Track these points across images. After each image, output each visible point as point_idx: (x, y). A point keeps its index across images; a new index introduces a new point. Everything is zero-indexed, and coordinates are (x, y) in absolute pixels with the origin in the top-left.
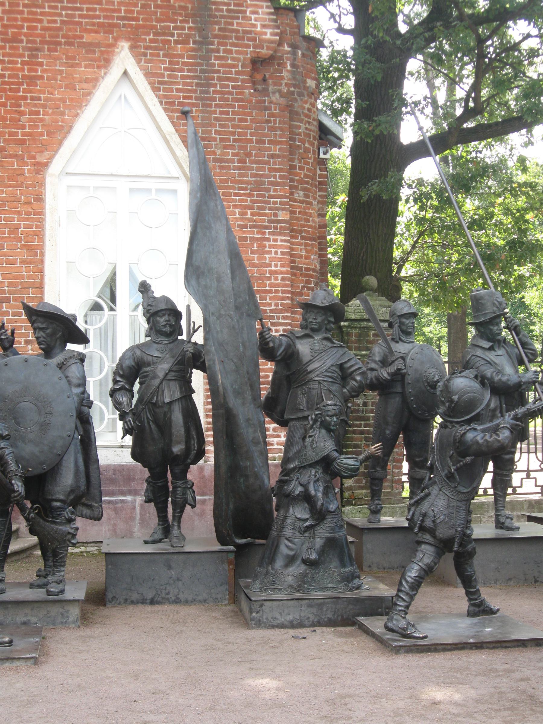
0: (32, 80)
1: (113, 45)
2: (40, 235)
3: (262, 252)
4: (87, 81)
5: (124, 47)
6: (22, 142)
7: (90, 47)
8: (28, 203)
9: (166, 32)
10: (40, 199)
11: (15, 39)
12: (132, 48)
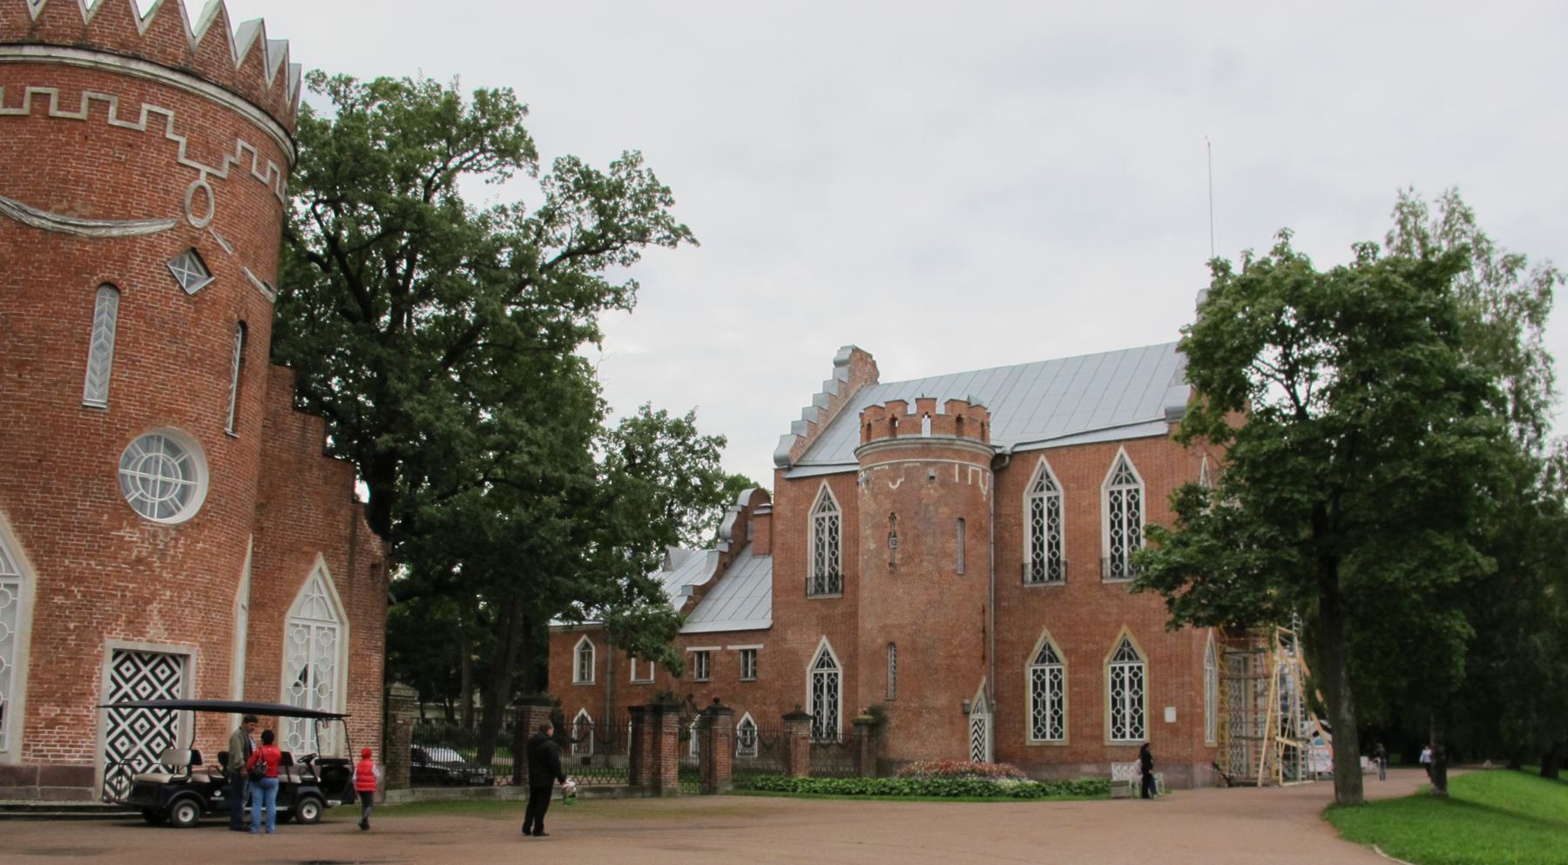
0: (281, 569)
1: (315, 554)
2: (280, 648)
3: (370, 661)
4: (303, 571)
5: (320, 554)
6: (274, 600)
7: (306, 554)
8: (275, 631)
9: (337, 549)
10: (281, 630)
11: (275, 547)
12: (324, 555)
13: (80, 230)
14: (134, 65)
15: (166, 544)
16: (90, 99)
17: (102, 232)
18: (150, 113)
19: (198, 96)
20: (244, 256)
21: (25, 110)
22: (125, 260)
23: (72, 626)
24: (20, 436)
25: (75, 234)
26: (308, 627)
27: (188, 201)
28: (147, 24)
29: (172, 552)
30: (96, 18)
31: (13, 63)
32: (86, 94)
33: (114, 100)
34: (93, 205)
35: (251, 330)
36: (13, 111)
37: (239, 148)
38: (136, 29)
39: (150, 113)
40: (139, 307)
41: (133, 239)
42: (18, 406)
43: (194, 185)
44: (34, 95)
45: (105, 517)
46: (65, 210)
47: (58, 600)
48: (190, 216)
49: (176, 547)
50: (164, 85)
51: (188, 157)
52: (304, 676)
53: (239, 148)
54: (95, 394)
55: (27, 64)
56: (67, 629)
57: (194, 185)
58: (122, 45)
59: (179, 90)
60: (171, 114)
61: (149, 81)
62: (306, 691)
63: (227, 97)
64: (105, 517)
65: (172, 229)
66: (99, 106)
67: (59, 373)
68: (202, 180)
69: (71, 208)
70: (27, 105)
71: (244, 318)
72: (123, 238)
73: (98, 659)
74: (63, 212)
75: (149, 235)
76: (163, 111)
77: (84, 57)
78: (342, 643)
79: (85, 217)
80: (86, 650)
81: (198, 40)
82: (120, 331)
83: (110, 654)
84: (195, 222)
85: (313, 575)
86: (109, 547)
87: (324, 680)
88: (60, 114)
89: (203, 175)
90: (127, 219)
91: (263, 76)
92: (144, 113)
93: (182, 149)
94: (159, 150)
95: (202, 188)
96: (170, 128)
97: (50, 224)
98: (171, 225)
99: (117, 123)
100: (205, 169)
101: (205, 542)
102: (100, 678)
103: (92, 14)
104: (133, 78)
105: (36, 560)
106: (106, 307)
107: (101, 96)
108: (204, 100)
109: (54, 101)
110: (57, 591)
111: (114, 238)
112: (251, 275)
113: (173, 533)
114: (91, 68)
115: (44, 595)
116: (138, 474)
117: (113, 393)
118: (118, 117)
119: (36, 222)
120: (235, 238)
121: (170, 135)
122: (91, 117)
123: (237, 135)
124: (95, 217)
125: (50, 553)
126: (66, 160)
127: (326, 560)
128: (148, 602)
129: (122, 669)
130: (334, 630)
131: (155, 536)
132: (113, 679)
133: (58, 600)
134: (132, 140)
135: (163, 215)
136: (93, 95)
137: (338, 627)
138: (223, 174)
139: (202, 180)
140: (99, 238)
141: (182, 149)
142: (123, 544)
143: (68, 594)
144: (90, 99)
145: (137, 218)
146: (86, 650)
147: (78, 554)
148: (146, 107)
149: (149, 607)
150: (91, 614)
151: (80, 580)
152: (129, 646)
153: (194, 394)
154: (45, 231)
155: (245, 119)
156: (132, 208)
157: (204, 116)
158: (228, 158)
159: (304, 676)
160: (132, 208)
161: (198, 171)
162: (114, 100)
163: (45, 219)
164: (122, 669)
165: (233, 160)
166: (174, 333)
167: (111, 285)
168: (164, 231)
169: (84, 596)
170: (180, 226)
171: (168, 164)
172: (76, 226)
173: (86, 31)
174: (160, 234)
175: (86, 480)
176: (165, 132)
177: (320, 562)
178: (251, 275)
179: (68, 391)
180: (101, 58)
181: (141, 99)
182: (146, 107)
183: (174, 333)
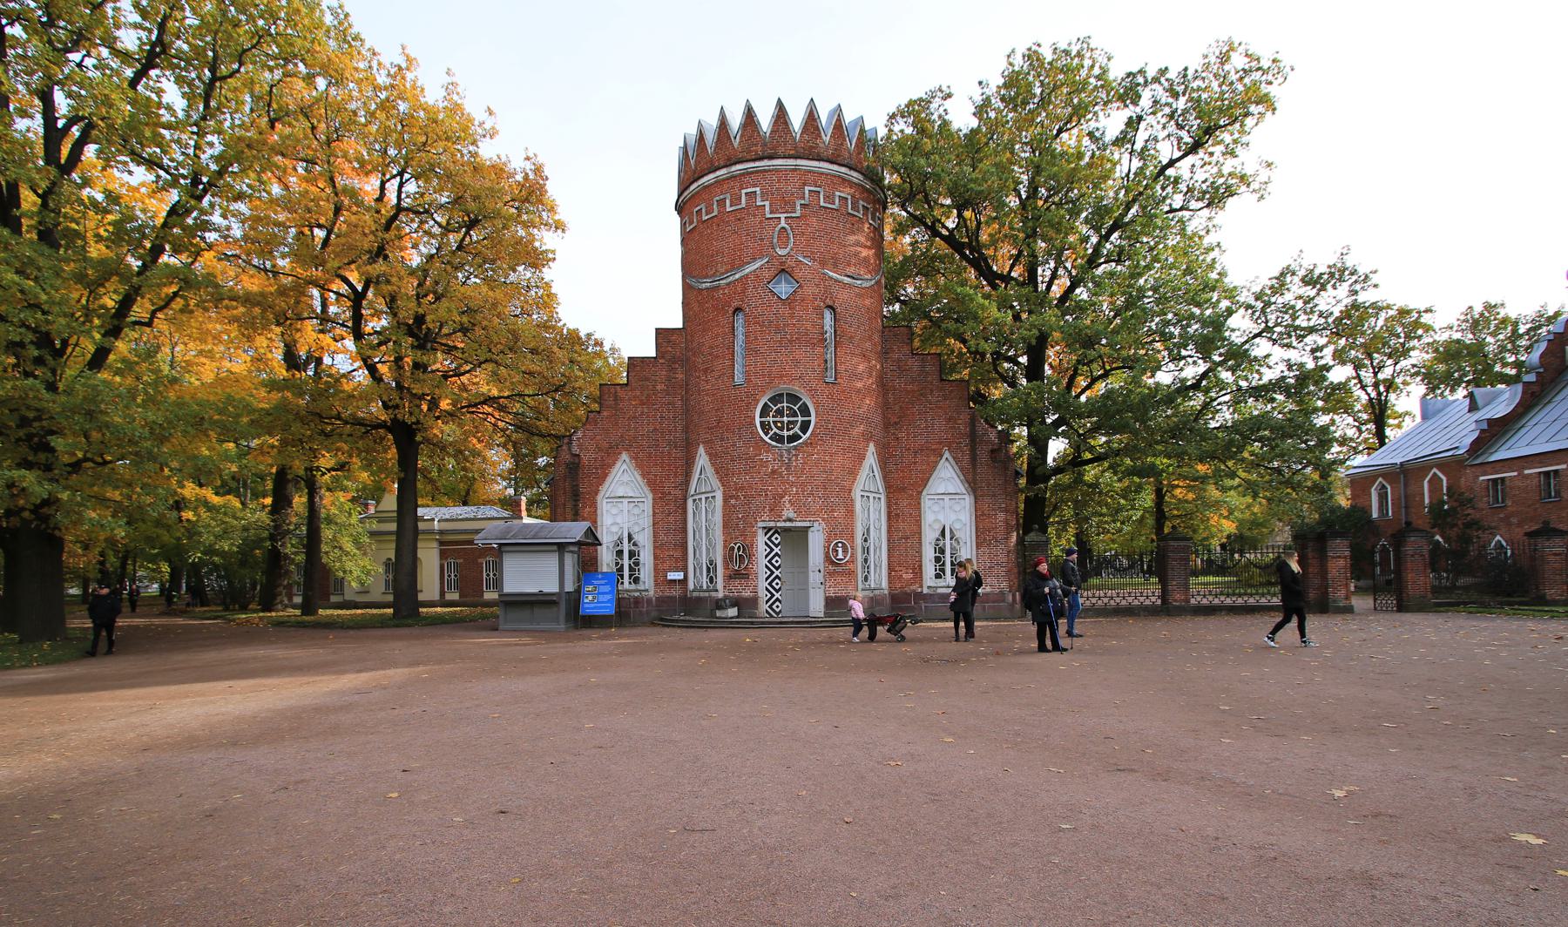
14: (734, 168)
15: (789, 460)
17: (731, 279)
19: (773, 170)
20: (823, 264)
22: (744, 290)
27: (775, 241)
28: (738, 137)
33: (728, 196)
35: (838, 310)
37: (807, 192)
42: (707, 395)
43: (777, 229)
47: (733, 502)
48: (778, 250)
49: (797, 460)
50: (752, 173)
53: (807, 192)
54: (739, 378)
56: (738, 518)
57: (777, 229)
58: (729, 159)
60: (758, 189)
63: (791, 162)
66: (722, 203)
68: (783, 223)
71: (829, 302)
72: (741, 278)
73: (755, 534)
74: (714, 275)
75: (755, 271)
76: (754, 189)
79: (723, 274)
81: (768, 134)
84: (780, 252)
89: (783, 221)
90: (742, 266)
91: (821, 137)
92: (743, 195)
93: (767, 209)
94: (755, 216)
95: (783, 228)
96: (759, 199)
100: (783, 216)
101: (818, 454)
104: (735, 177)
106: (740, 321)
107: (722, 197)
108: (777, 171)
112: (831, 274)
113: (794, 452)
114: (716, 182)
115: (726, 500)
116: (771, 419)
117: (747, 374)
119: (704, 285)
120: (812, 253)
122: (719, 212)
123: (805, 184)
126: (712, 244)
131: (782, 456)
133: (733, 502)
134: (739, 216)
136: (718, 198)
138: (798, 214)
139: (783, 223)
140: (730, 283)
141: (767, 209)
142: (764, 464)
143: (737, 498)
145: (750, 263)
148: (744, 191)
151: (742, 488)
152: (772, 524)
153: (797, 362)
154: (707, 288)
155: (810, 172)
157: (779, 181)
158: (798, 203)
164: (773, 539)
165: (803, 202)
166: (777, 327)
167: (738, 310)
170: (772, 258)
171: (761, 222)
173: (711, 161)
178: (831, 274)
180: (718, 173)
183: (777, 327)
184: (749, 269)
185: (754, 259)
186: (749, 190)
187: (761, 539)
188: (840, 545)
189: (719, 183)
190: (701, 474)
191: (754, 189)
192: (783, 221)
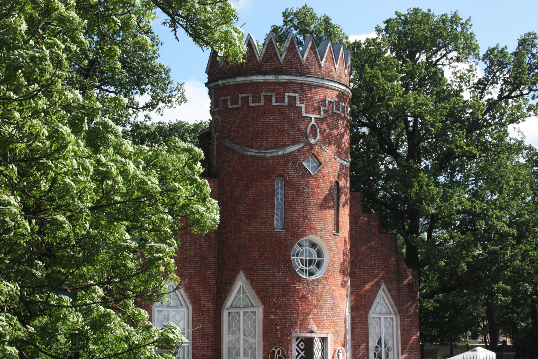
2: (367, 329)
10: (367, 321)
12: (384, 282)
13: (266, 154)
14: (280, 77)
16: (264, 96)
18: (289, 97)
21: (240, 105)
22: (285, 164)
23: (278, 328)
24: (251, 247)
25: (264, 157)
26: (380, 318)
29: (316, 292)
30: (263, 59)
31: (233, 85)
32: (263, 94)
33: (274, 94)
34: (270, 143)
36: (235, 106)
38: (279, 60)
39: (289, 97)
40: (293, 184)
41: (288, 155)
44: (242, 98)
45: (288, 279)
46: (260, 146)
47: (272, 317)
49: (318, 289)
50: (293, 83)
51: (306, 113)
52: (380, 342)
55: (238, 86)
56: (277, 329)
58: (275, 69)
59: (299, 83)
61: (286, 83)
62: (381, 350)
64: (288, 279)
65: (303, 147)
66: (268, 99)
67: (263, 218)
68: (313, 122)
69: (262, 145)
70: (240, 103)
73: (290, 342)
75: (294, 152)
76: (294, 95)
77: (260, 78)
78: (397, 325)
79: (268, 149)
80: (285, 338)
82: (286, 195)
83: (294, 340)
85: (381, 292)
86: (290, 292)
87: (390, 344)
88: (253, 105)
89: (313, 120)
93: (303, 110)
94: (294, 113)
96: (298, 102)
97: (254, 154)
98: (302, 145)
99: (276, 104)
100: (313, 116)
102: (291, 350)
103: (261, 58)
105: (262, 299)
107: (268, 94)
109: (250, 99)
110: (272, 313)
111: (280, 156)
118: (276, 102)
121: (297, 105)
124: (271, 148)
125: (267, 297)
127: (385, 284)
128: (308, 315)
129: (300, 345)
130: (392, 318)
132: (297, 350)
133: (272, 317)
134: (282, 111)
135: (298, 142)
136: (265, 94)
137: (394, 317)
139: (313, 122)
140: (274, 157)
143: (276, 314)
144: (264, 96)
145: (289, 145)
146: (285, 338)
147: (278, 296)
148: (287, 94)
149: (309, 317)
150: (285, 322)
151: (280, 307)
154: (252, 157)
156: (286, 141)
159: (380, 342)
160: (286, 141)
161: (311, 118)
162: (274, 94)
163: (252, 152)
165: (325, 108)
168: (299, 149)
169: (282, 314)
171: (298, 118)
172: (264, 153)
174: (298, 150)
175: (279, 263)
176: (295, 103)
177: (383, 286)
179: (268, 225)
181: (285, 92)
182: (287, 94)
184: (290, 149)
185: (293, 144)
186: (291, 94)
187: (294, 346)
188: (341, 351)
189: (266, 84)
190: (238, 293)
191: (294, 95)
192: (313, 120)
